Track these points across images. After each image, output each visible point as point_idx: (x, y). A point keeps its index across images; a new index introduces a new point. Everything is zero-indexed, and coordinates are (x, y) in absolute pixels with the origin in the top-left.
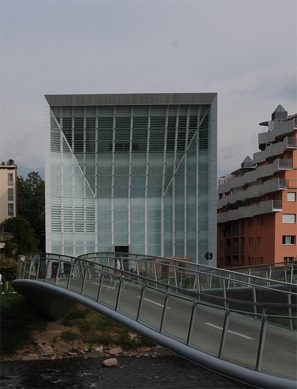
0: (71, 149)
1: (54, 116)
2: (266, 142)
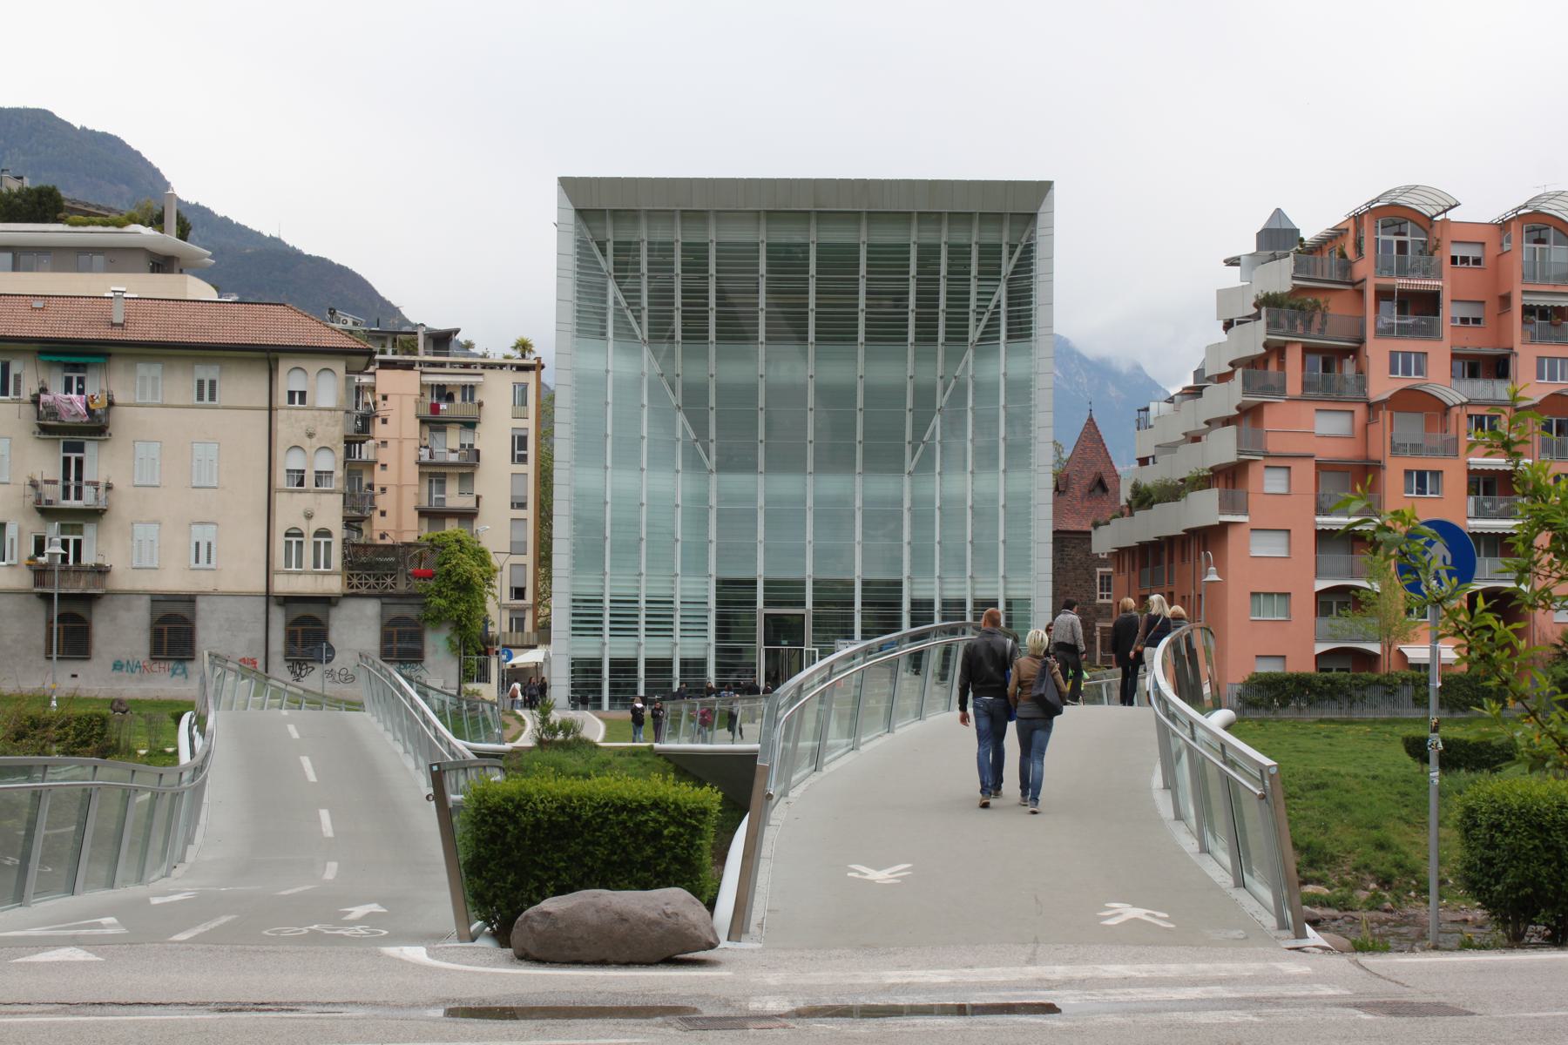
0: (638, 331)
1: (589, 237)
2: (1236, 314)
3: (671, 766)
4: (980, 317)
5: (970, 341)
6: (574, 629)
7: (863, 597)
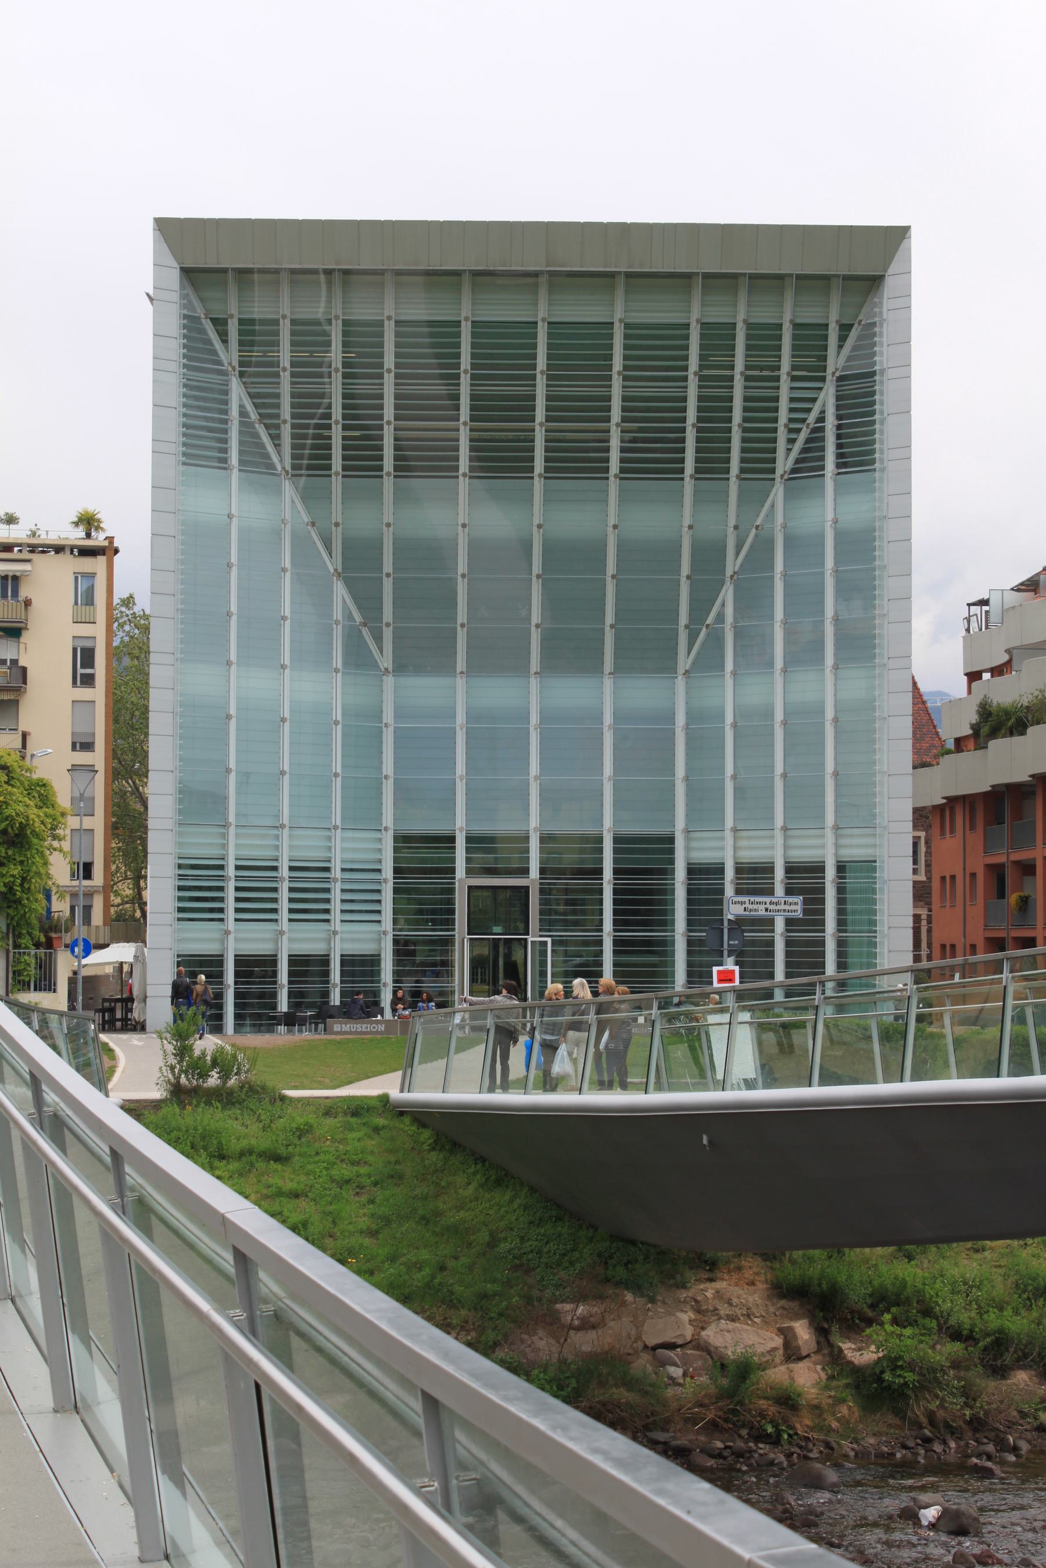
1: (200, 312)
3: (426, 1134)
4: (793, 436)
5: (779, 471)
6: (180, 910)
7: (615, 861)
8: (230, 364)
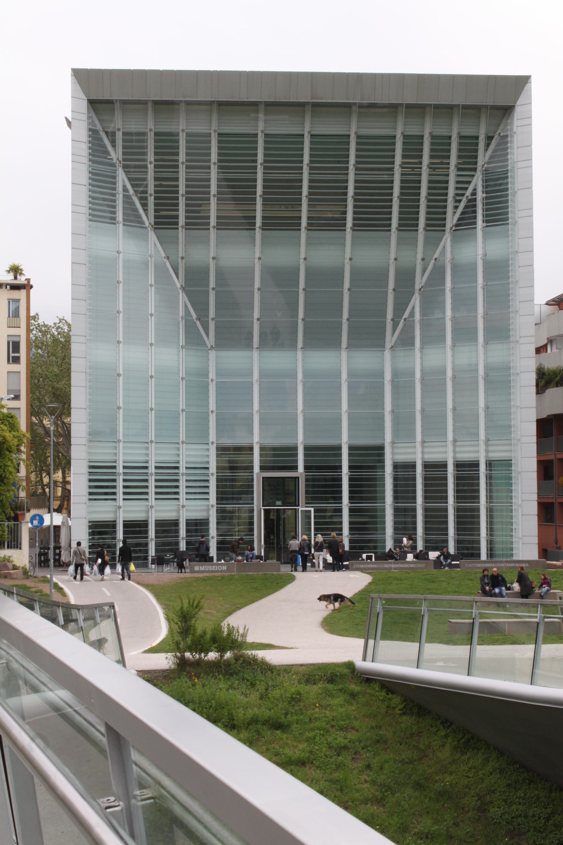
1: (99, 127)
3: (396, 700)
4: (457, 204)
6: (90, 494)
7: (350, 461)
8: (118, 159)
